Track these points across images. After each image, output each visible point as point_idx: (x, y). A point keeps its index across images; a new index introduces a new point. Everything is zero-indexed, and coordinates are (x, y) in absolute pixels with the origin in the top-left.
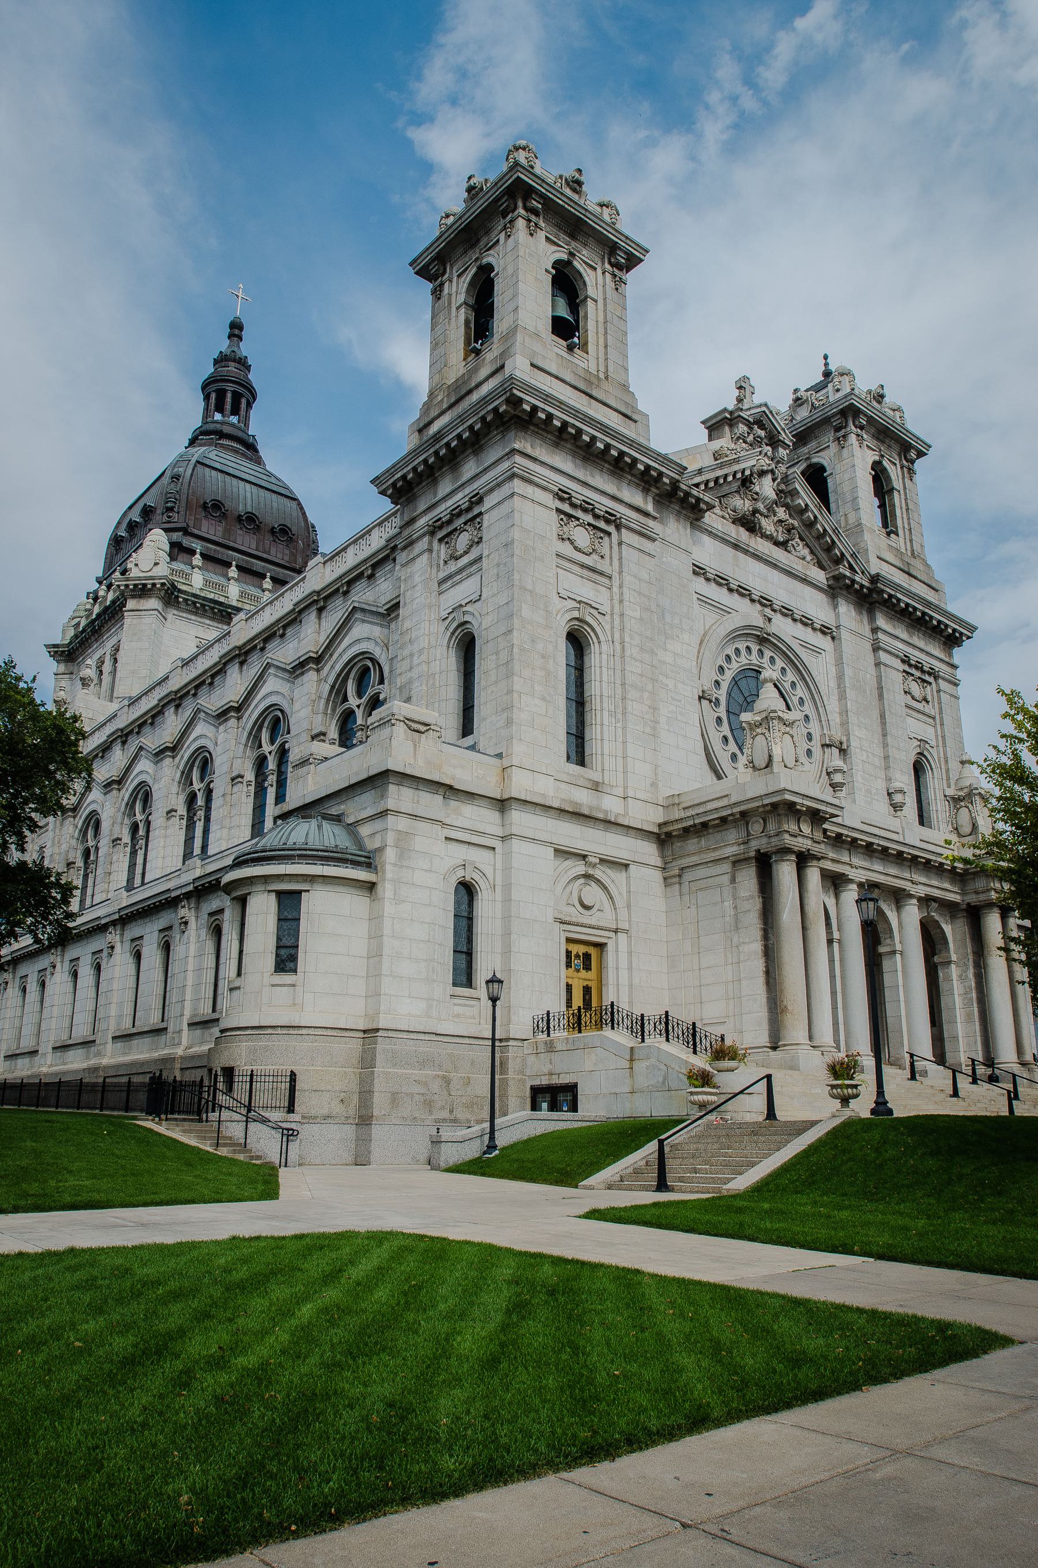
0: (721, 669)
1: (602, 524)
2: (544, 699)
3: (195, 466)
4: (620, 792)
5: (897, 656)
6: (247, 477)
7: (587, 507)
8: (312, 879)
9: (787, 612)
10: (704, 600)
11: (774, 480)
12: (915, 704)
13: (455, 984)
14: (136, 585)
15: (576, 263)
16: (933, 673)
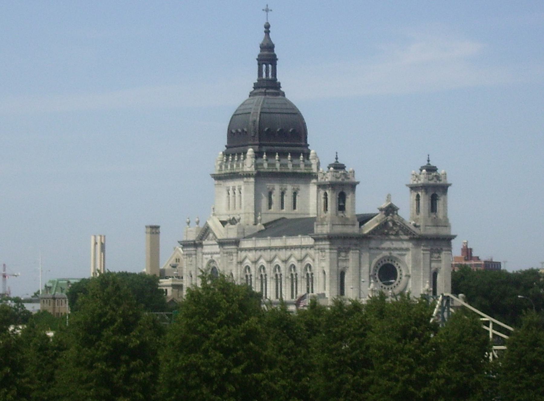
3: (260, 115)
6: (279, 111)
7: (344, 248)
12: (435, 259)
15: (344, 191)
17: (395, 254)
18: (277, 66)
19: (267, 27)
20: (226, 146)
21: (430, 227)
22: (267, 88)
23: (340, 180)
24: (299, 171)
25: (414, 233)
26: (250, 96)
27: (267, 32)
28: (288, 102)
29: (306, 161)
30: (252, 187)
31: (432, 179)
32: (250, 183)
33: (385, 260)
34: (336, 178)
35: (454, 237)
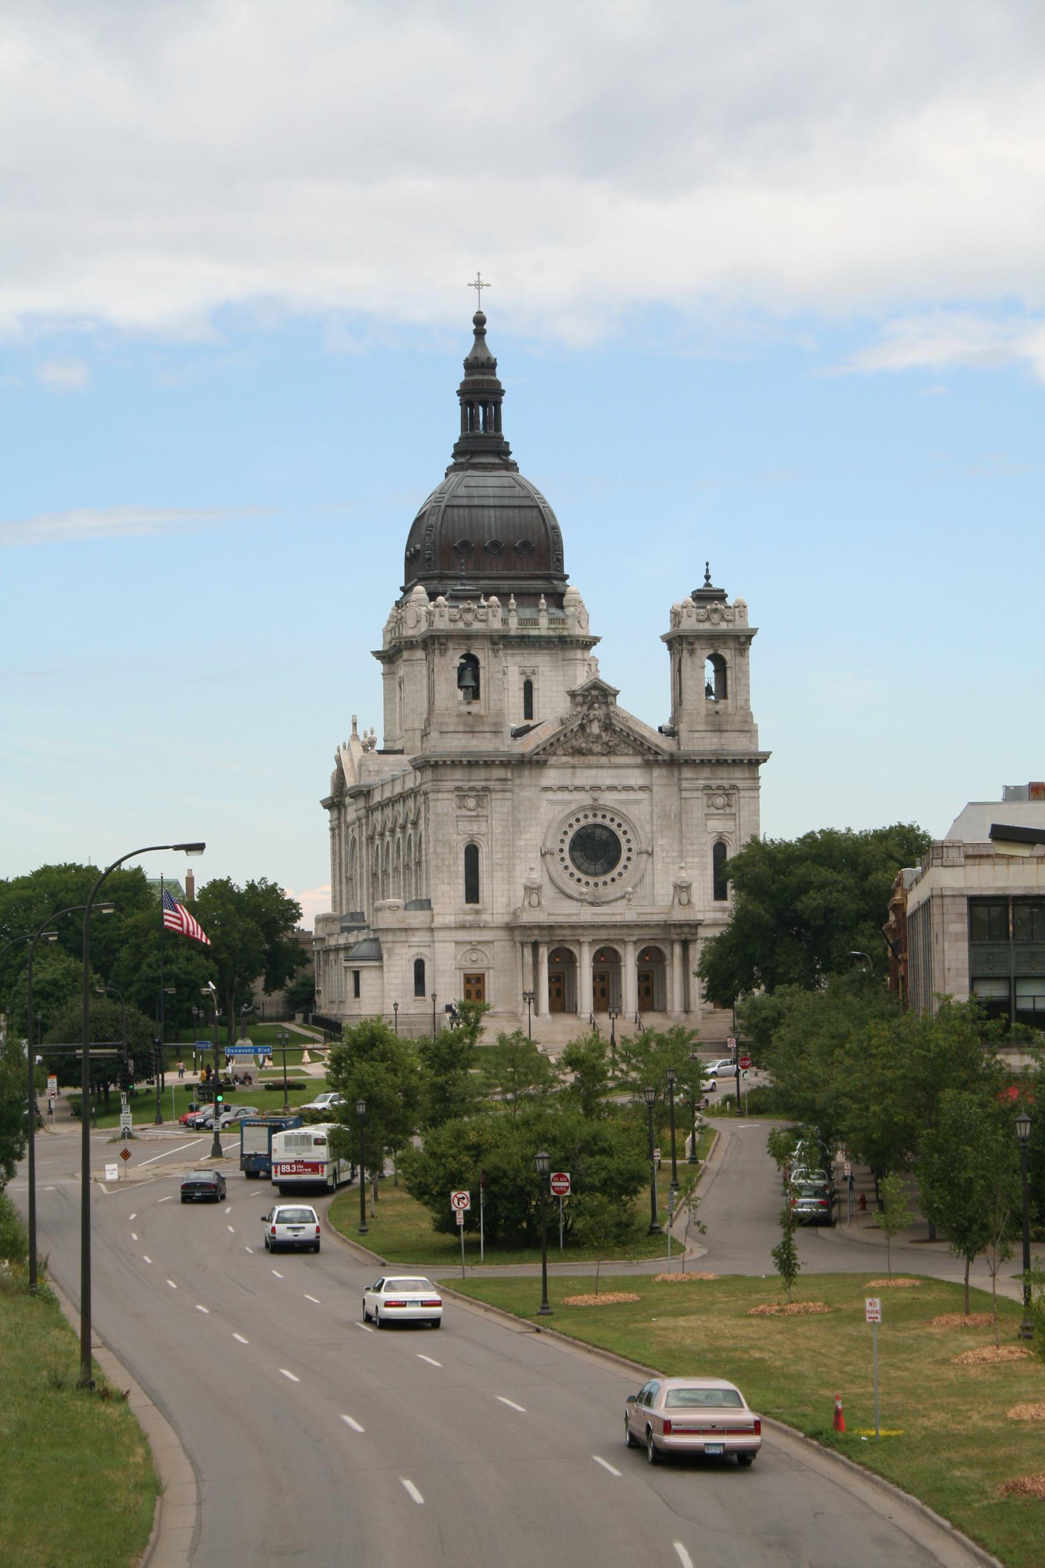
0: (565, 833)
1: (482, 793)
2: (449, 884)
3: (445, 511)
4: (490, 912)
5: (698, 790)
6: (491, 502)
7: (471, 789)
8: (362, 967)
9: (612, 788)
10: (551, 802)
11: (599, 721)
12: (716, 811)
13: (416, 995)
14: (406, 642)
15: (473, 652)
16: (734, 787)
17: (608, 799)
18: (503, 407)
19: (480, 321)
20: (402, 589)
21: (703, 734)
22: (473, 453)
23: (461, 625)
24: (534, 633)
25: (654, 748)
26: (447, 475)
27: (480, 333)
28: (521, 484)
29: (553, 610)
30: (422, 670)
31: (708, 619)
32: (414, 662)
33: (586, 816)
34: (451, 620)
35: (765, 757)
